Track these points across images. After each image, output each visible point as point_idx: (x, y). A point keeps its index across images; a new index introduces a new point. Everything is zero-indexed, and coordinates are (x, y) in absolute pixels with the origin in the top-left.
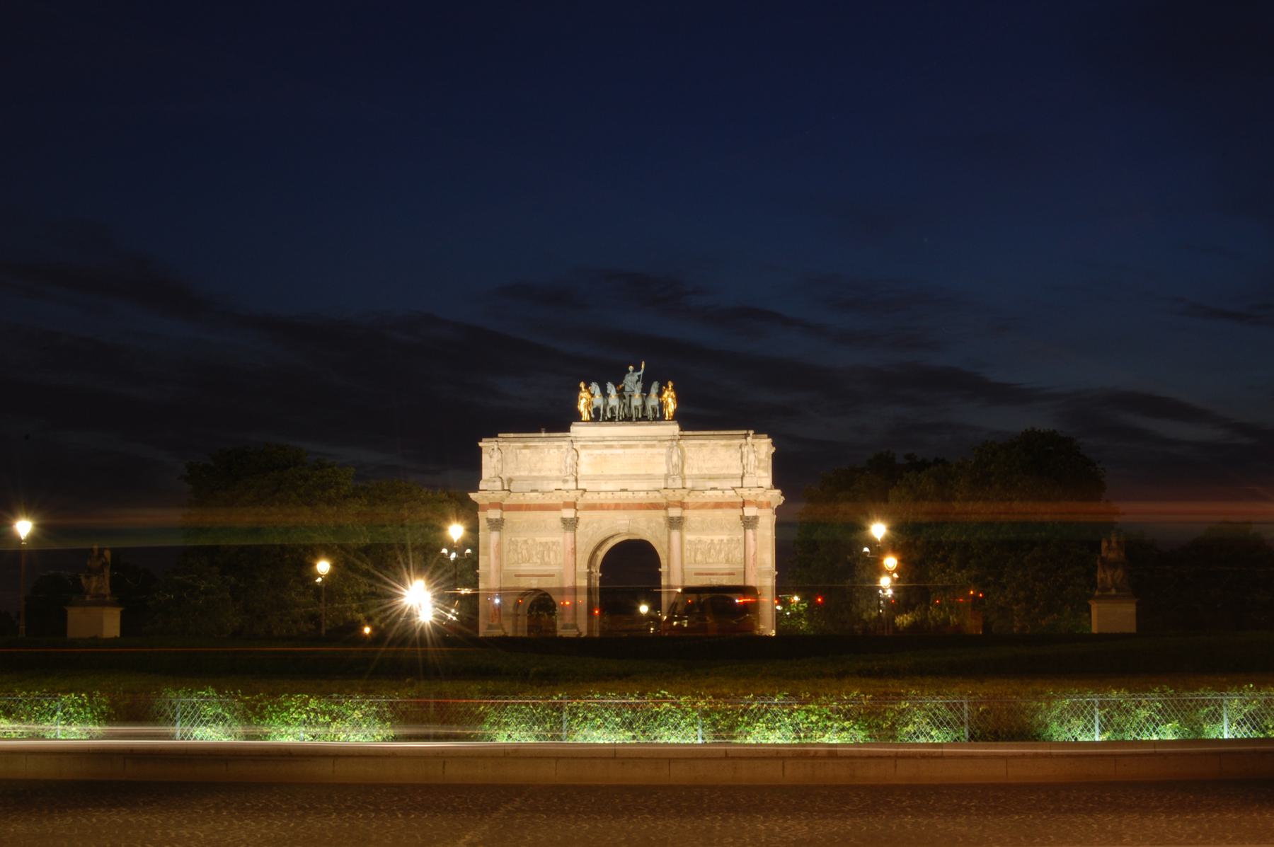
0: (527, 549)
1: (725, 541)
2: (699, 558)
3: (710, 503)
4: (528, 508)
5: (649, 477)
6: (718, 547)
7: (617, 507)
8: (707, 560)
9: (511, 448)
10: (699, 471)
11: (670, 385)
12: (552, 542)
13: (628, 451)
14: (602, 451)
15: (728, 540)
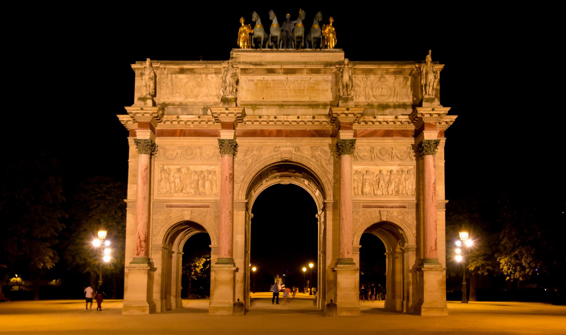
0: (180, 177)
1: (395, 172)
2: (367, 189)
3: (379, 130)
4: (183, 133)
5: (313, 105)
6: (387, 178)
7: (279, 134)
8: (375, 192)
9: (165, 72)
10: (366, 98)
11: (331, 20)
12: (207, 170)
13: (291, 77)
14: (263, 77)
15: (398, 171)
